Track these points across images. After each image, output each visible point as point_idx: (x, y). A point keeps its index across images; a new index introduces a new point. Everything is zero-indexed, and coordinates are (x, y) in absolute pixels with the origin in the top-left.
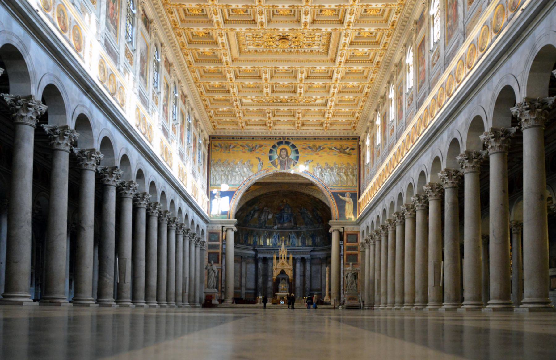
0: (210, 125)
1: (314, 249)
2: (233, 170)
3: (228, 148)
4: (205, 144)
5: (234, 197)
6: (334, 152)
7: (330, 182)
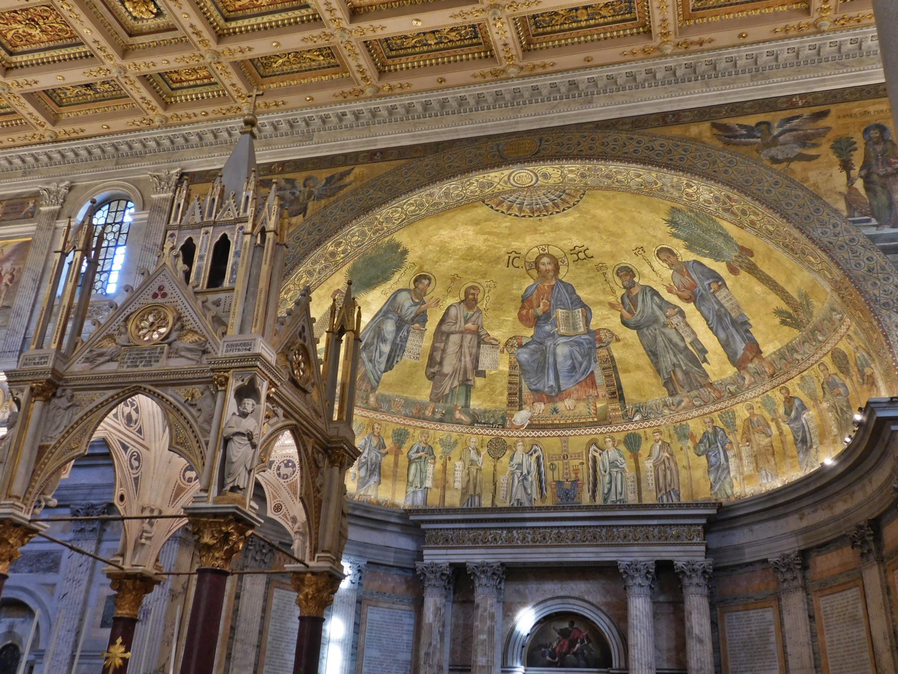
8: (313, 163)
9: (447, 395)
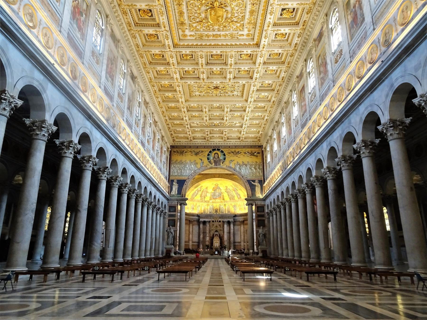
0: (171, 140)
2: (185, 166)
3: (182, 153)
4: (168, 151)
5: (185, 183)
6: (247, 155)
7: (245, 174)
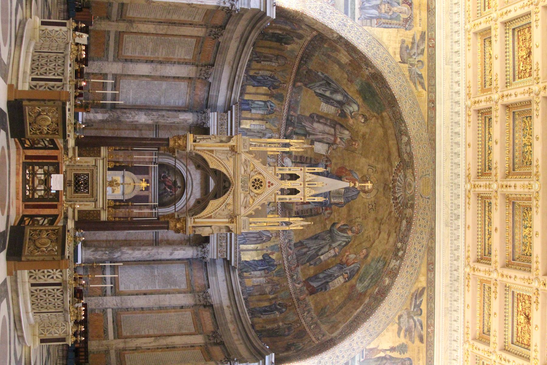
1: (235, 268)
8: (432, 66)
9: (301, 124)
